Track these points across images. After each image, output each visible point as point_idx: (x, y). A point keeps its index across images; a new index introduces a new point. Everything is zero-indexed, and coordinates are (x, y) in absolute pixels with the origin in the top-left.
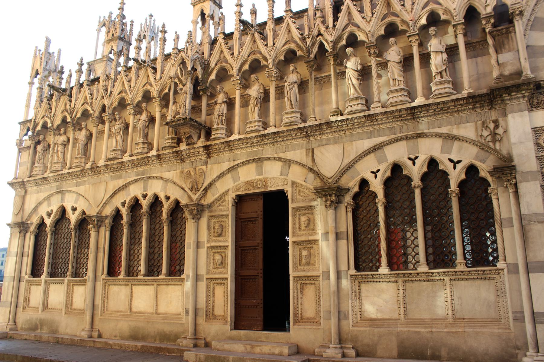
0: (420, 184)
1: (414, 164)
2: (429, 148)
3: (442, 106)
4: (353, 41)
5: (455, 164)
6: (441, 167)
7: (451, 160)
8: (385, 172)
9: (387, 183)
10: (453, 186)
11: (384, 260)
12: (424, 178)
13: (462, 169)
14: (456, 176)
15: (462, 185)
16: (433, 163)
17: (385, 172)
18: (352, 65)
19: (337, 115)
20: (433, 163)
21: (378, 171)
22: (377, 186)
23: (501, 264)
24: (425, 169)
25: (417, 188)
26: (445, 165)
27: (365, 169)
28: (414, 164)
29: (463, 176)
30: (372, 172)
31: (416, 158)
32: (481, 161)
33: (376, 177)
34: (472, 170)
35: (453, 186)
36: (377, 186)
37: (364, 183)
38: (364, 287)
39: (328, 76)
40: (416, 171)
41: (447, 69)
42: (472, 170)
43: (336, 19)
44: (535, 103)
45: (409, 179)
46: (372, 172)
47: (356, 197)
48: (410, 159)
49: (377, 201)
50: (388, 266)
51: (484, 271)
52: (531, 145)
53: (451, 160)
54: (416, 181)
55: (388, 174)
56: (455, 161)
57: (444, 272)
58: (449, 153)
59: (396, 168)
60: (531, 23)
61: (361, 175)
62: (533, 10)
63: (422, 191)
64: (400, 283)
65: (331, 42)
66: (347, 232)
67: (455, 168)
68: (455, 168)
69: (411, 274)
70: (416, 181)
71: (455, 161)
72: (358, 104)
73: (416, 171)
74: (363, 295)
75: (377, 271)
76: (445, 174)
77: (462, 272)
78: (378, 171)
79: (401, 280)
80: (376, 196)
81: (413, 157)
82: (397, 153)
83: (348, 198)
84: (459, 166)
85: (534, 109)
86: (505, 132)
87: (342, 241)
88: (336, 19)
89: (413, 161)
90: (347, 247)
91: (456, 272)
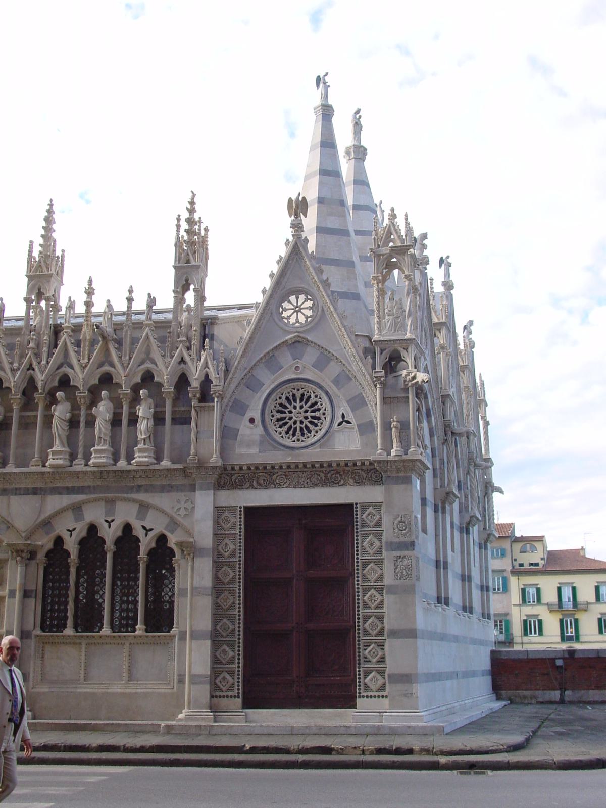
0: (112, 547)
1: (110, 527)
2: (125, 513)
3: (141, 473)
4: (65, 383)
5: (147, 531)
6: (134, 533)
7: (144, 528)
8: (81, 532)
9: (82, 543)
10: (143, 554)
11: (70, 622)
12: (118, 542)
13: (153, 537)
14: (146, 544)
15: (151, 553)
16: (127, 528)
17: (81, 531)
18: (61, 411)
19: (38, 465)
20: (127, 528)
21: (74, 529)
22: (71, 545)
23: (174, 631)
24: (119, 533)
25: (109, 551)
26: (139, 532)
27: (61, 528)
28: (110, 527)
29: (153, 545)
30: (69, 530)
31: (113, 521)
32: (170, 531)
33: (71, 535)
34: (162, 539)
35: (143, 554)
36: (71, 545)
37: (59, 541)
38: (48, 648)
39: (35, 416)
40: (110, 534)
41: (152, 436)
42: (162, 539)
43: (50, 354)
44: (222, 483)
45: (103, 542)
46: (69, 530)
47: (48, 555)
48: (106, 521)
49: (69, 561)
50: (74, 628)
51: (159, 637)
52: (210, 523)
53: (144, 528)
54: (110, 546)
55: (84, 534)
56: (148, 528)
57: (125, 637)
58: (143, 519)
59: (93, 529)
60: (231, 404)
61: (55, 533)
62: (234, 392)
63: (115, 555)
64: (83, 647)
65: (42, 381)
66: (36, 590)
67: (146, 535)
68: (146, 535)
69: (93, 637)
70: (110, 546)
71: (148, 528)
72: (60, 458)
73: (110, 534)
74: (46, 656)
75: (62, 632)
76: (138, 540)
77: (141, 637)
78: (74, 529)
79: (84, 642)
80: (69, 555)
81: (109, 520)
82: (94, 514)
83: (41, 556)
84: (151, 534)
85: (220, 488)
86: (193, 508)
87: (30, 599)
88: (50, 354)
89: (109, 523)
90: (34, 606)
91: (135, 637)
